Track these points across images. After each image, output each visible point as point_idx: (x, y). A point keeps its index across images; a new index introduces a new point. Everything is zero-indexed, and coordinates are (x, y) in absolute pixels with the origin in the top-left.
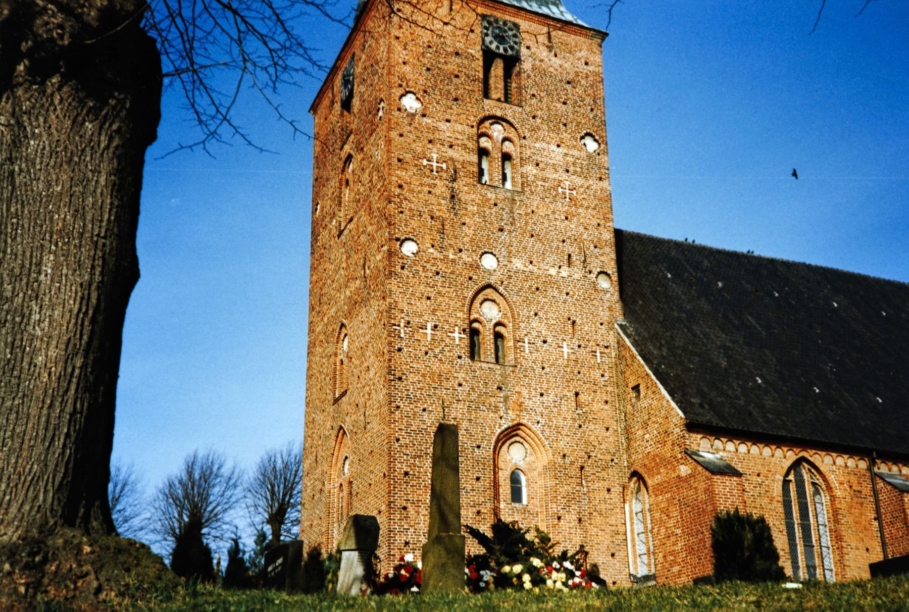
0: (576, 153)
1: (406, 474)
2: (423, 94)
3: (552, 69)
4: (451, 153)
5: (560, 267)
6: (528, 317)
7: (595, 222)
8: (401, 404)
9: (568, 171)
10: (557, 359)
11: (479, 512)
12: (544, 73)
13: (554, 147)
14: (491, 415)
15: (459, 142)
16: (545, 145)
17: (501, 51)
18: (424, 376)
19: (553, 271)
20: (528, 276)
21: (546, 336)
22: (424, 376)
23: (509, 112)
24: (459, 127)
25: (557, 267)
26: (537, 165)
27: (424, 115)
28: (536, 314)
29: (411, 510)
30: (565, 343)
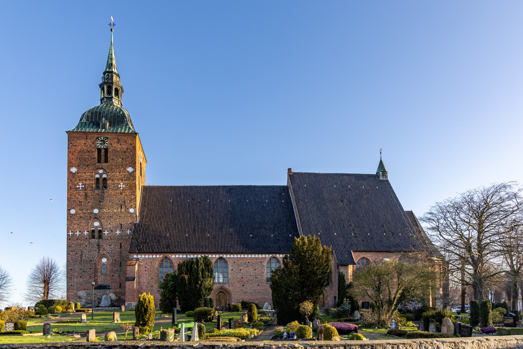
0: (125, 174)
1: (71, 269)
2: (78, 167)
3: (118, 149)
4: (85, 182)
5: (118, 209)
6: (107, 225)
8: (70, 253)
9: (122, 180)
10: (115, 235)
11: (91, 277)
12: (117, 151)
14: (95, 252)
15: (88, 178)
16: (115, 173)
17: (102, 147)
18: (76, 245)
19: (115, 211)
21: (112, 229)
22: (76, 245)
23: (105, 165)
24: (88, 174)
25: (117, 209)
26: (112, 180)
27: (78, 173)
28: (110, 224)
29: (72, 277)
30: (118, 230)
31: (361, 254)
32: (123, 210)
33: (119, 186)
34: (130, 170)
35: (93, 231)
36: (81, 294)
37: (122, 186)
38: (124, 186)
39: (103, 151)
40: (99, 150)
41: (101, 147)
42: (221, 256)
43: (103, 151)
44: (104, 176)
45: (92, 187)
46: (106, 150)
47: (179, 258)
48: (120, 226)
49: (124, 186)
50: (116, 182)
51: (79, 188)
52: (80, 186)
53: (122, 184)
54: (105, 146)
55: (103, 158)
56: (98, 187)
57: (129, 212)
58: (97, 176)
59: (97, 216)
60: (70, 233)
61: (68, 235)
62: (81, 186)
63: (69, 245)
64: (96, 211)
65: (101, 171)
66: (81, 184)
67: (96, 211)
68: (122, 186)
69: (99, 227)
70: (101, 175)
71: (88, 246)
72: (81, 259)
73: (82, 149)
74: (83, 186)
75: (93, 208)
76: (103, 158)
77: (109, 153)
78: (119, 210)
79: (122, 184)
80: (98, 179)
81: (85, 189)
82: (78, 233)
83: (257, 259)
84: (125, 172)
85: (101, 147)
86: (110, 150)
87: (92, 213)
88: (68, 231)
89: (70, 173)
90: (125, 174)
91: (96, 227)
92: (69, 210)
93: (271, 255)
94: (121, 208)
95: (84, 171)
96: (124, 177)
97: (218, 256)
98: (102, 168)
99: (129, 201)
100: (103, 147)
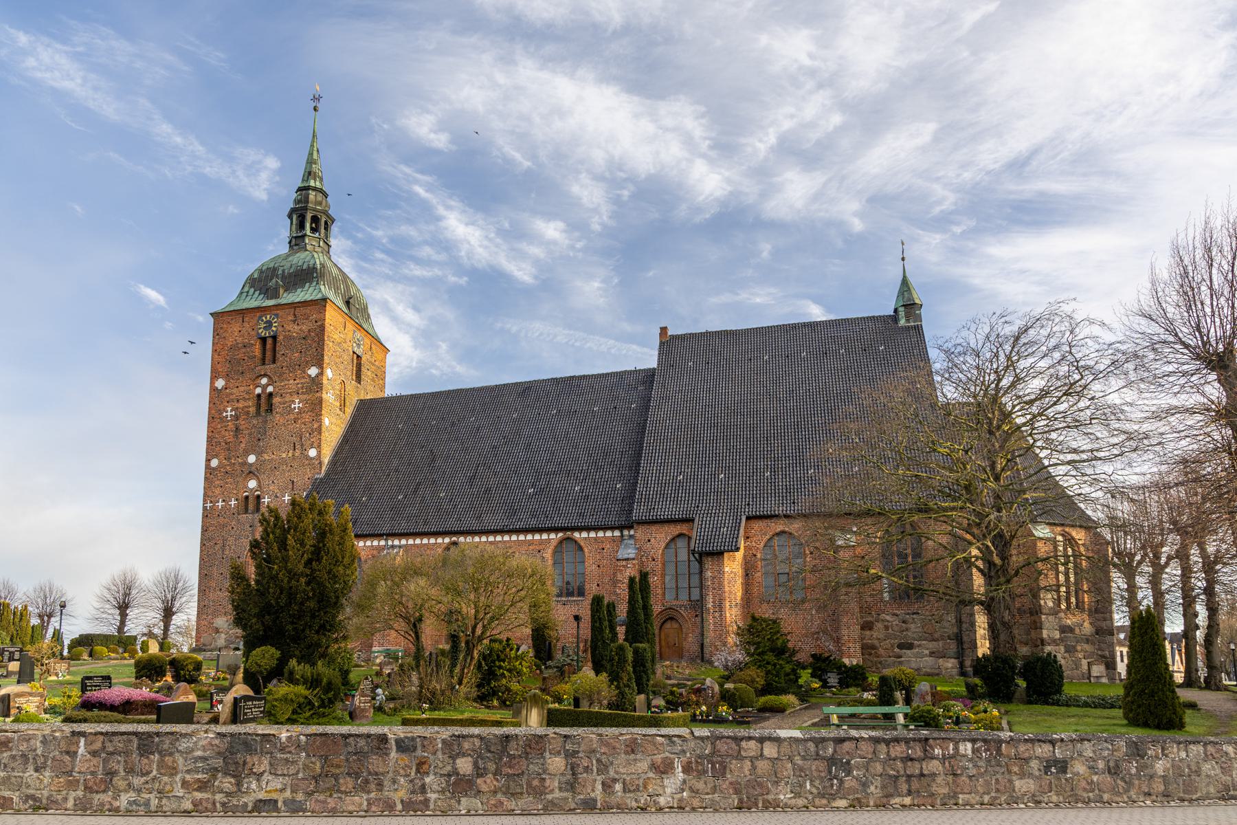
0: (303, 381)
2: (227, 377)
3: (294, 334)
4: (237, 405)
7: (311, 418)
13: (292, 382)
16: (286, 382)
17: (267, 335)
19: (284, 455)
20: (271, 461)
23: (269, 368)
31: (773, 524)
32: (298, 453)
33: (293, 406)
34: (313, 371)
35: (247, 497)
36: (219, 623)
37: (297, 406)
38: (301, 405)
39: (269, 341)
40: (264, 340)
41: (265, 334)
42: (454, 539)
43: (269, 341)
44: (270, 389)
45: (248, 413)
46: (274, 338)
47: (372, 546)
48: (290, 486)
49: (301, 405)
50: (288, 398)
51: (227, 416)
52: (229, 413)
53: (297, 401)
54: (273, 331)
55: (269, 354)
56: (258, 413)
57: (308, 458)
58: (258, 391)
59: (253, 469)
60: (208, 505)
61: (205, 508)
62: (229, 414)
63: (205, 528)
64: (252, 459)
65: (264, 381)
66: (229, 409)
67: (252, 459)
68: (297, 405)
69: (257, 491)
70: (264, 387)
71: (235, 529)
72: (223, 553)
73: (235, 342)
74: (233, 413)
75: (247, 453)
76: (269, 354)
77: (278, 344)
78: (290, 455)
79: (297, 401)
80: (259, 396)
81: (236, 418)
82: (220, 504)
83: (531, 543)
84: (304, 377)
85: (265, 334)
86: (281, 338)
87: (245, 463)
88: (205, 501)
89: (213, 389)
90: (303, 381)
91: (252, 490)
92: (208, 460)
93: (560, 535)
94: (294, 449)
95: (237, 384)
96: (302, 388)
97: (447, 540)
98: (265, 375)
99: (308, 435)
100: (269, 333)
